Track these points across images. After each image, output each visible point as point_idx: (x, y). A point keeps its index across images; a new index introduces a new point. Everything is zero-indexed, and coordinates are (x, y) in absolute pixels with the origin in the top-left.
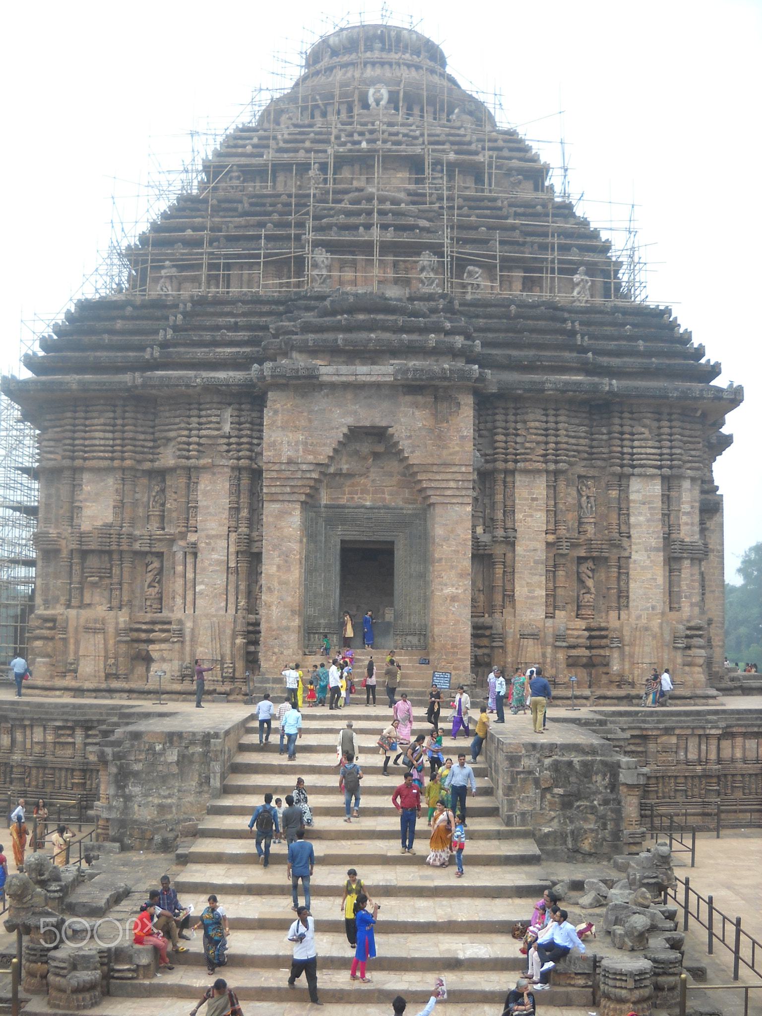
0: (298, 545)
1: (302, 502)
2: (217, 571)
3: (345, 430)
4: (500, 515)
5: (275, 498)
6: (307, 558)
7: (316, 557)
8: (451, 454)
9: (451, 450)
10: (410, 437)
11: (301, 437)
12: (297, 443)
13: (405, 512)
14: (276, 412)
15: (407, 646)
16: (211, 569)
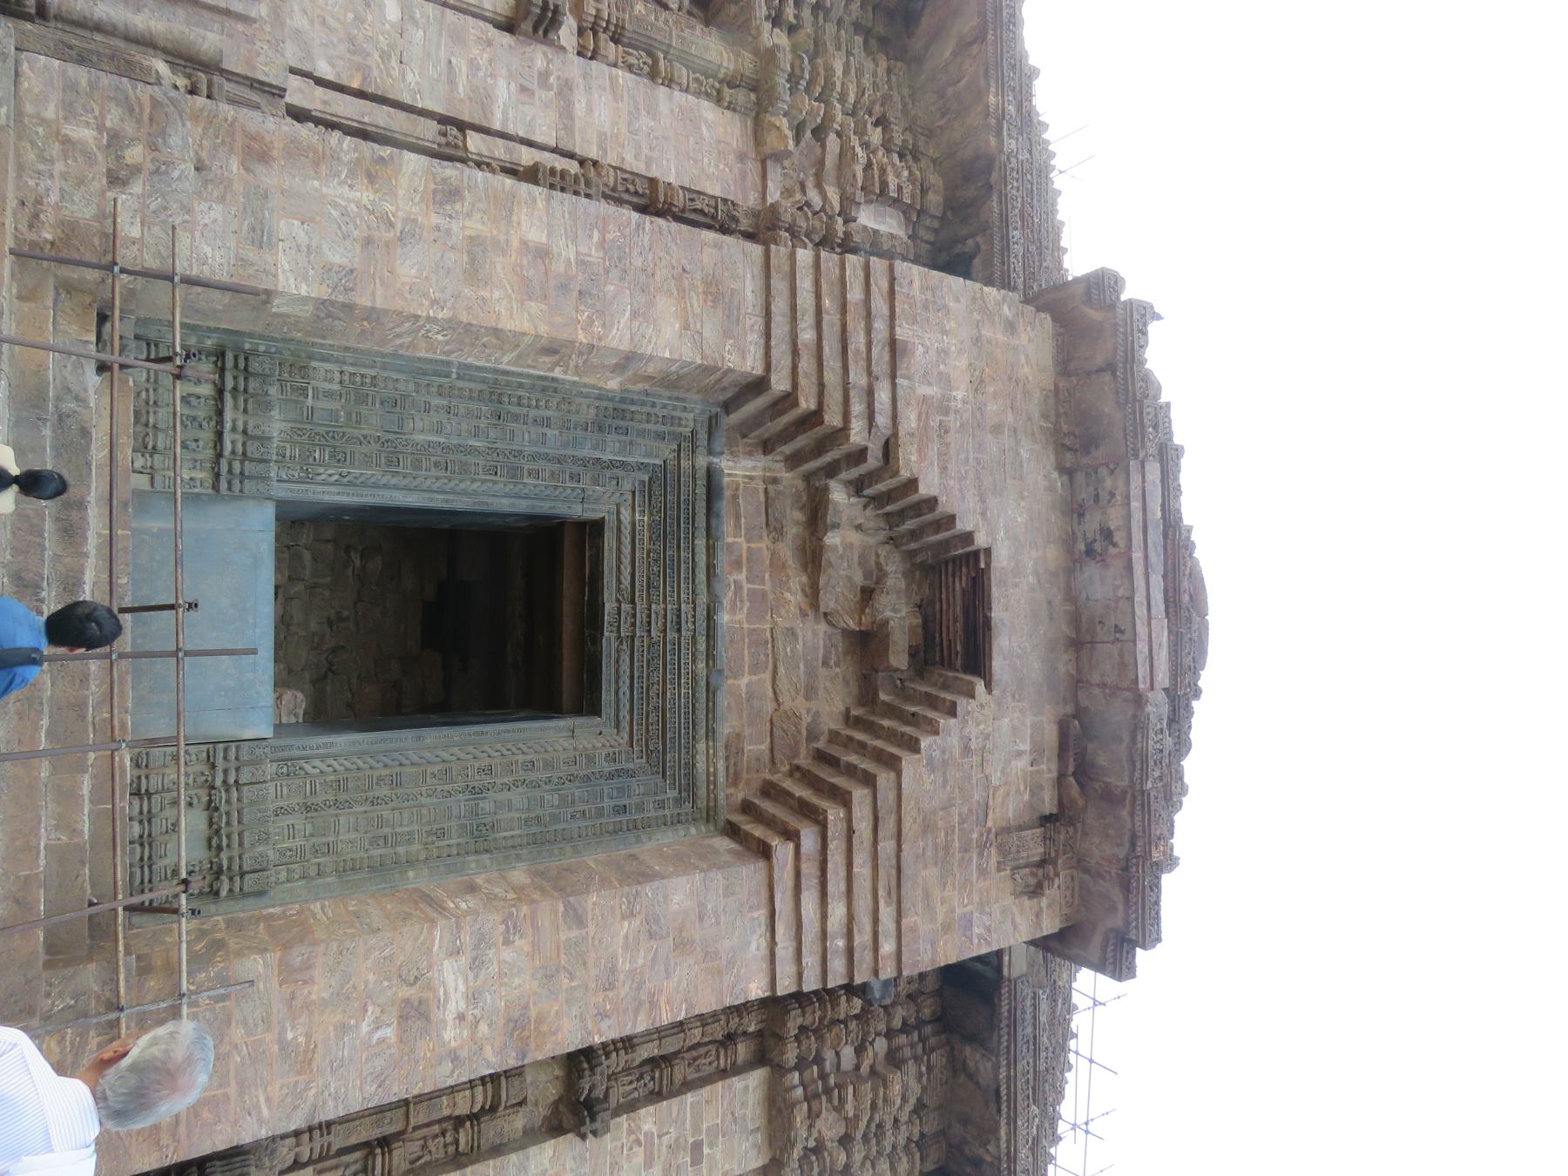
0: (625, 346)
1: (759, 385)
2: (452, 82)
3: (981, 540)
4: (644, 1052)
5: (779, 285)
6: (548, 387)
7: (547, 423)
8: (927, 895)
9: (937, 894)
10: (966, 750)
11: (959, 394)
12: (946, 381)
13: (701, 746)
14: (1011, 327)
15: (147, 818)
16: (461, 65)
